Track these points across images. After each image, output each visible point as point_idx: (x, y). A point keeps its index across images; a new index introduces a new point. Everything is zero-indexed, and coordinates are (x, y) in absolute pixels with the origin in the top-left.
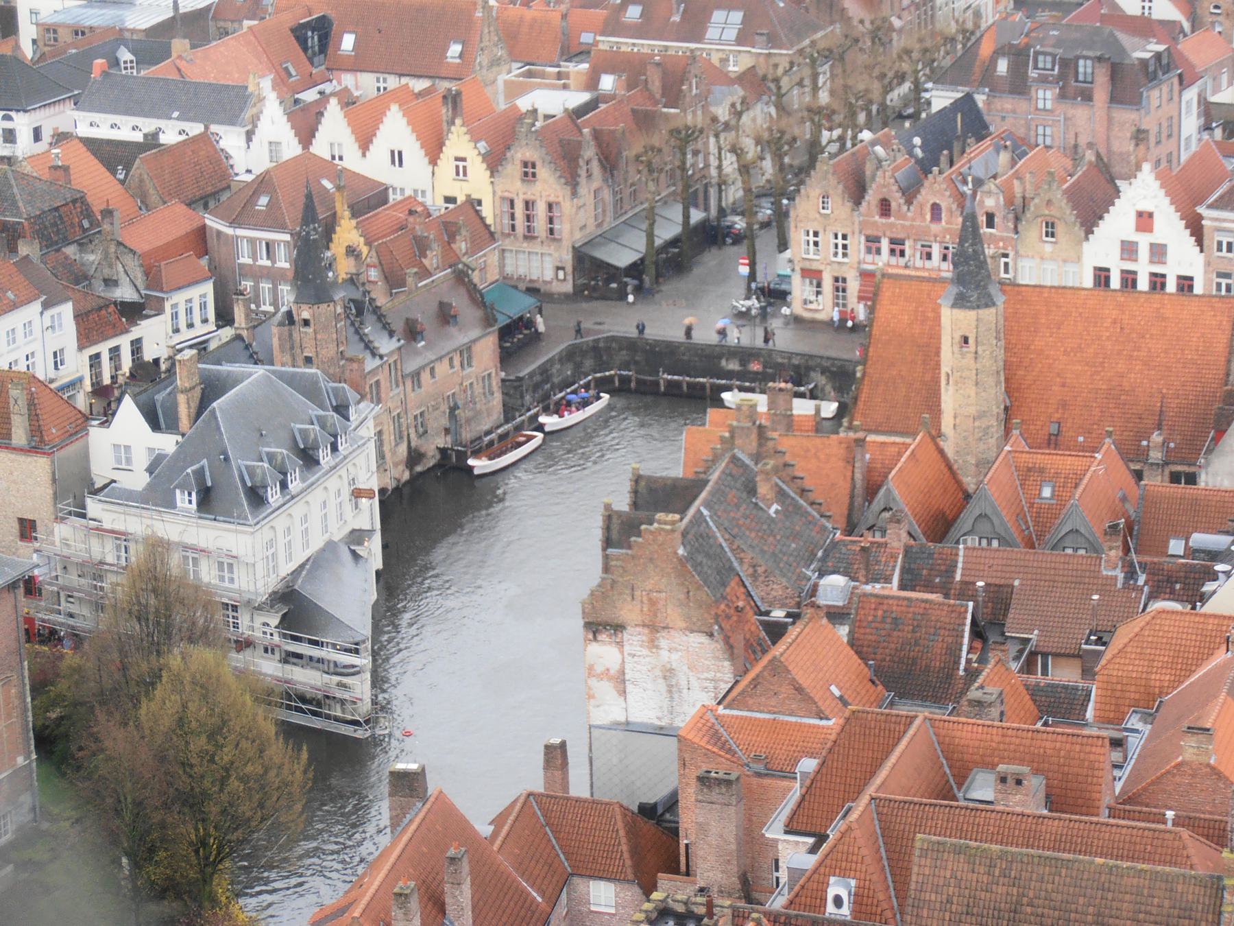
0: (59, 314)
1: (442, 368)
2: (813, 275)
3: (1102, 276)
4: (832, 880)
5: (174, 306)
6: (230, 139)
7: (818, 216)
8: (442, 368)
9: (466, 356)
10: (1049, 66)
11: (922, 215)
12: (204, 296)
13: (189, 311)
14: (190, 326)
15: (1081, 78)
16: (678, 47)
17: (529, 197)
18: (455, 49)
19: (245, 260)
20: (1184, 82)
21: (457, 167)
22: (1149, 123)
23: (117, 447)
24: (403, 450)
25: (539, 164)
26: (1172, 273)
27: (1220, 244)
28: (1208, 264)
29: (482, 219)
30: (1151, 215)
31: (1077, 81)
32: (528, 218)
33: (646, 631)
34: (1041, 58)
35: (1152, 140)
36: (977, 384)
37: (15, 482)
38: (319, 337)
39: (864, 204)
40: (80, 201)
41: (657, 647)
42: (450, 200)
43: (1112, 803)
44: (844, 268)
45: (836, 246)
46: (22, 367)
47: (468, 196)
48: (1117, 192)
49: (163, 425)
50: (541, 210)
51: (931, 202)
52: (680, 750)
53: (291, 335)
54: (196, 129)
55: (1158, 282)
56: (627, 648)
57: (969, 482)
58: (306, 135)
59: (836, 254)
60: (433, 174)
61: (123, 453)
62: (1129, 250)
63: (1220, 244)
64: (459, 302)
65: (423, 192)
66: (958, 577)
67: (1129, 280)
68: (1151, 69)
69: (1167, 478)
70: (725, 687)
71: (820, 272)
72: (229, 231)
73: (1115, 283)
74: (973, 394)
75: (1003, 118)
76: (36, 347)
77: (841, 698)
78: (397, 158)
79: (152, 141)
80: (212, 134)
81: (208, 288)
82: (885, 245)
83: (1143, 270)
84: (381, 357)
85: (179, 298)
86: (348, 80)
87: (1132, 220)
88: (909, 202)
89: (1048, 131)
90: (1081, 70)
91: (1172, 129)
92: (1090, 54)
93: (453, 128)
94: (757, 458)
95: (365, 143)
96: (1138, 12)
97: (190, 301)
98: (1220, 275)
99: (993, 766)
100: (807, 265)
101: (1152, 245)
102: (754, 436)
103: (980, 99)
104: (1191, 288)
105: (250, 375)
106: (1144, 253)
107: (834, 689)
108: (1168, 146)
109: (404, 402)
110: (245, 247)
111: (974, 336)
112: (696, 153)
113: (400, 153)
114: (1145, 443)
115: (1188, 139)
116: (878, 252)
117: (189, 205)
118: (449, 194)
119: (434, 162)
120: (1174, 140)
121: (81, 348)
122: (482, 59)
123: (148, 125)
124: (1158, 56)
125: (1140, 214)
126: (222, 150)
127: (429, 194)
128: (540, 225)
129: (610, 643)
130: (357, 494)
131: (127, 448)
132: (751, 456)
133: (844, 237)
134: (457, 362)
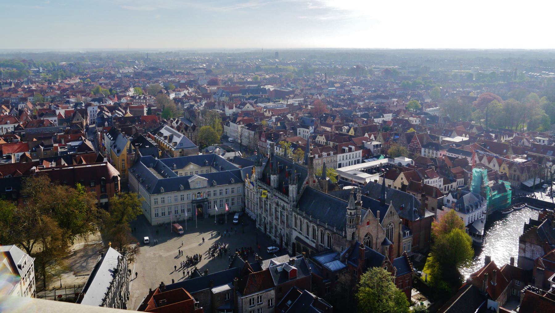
13: (460, 182)
16: (542, 155)
18: (505, 151)
23: (448, 200)
32: (514, 177)
40: (446, 165)
42: (502, 172)
46: (435, 186)
54: (464, 157)
61: (448, 201)
79: (457, 158)
85: (458, 180)
112: (543, 171)
121: (443, 185)
123: (457, 155)
130: (483, 213)
131: (449, 200)
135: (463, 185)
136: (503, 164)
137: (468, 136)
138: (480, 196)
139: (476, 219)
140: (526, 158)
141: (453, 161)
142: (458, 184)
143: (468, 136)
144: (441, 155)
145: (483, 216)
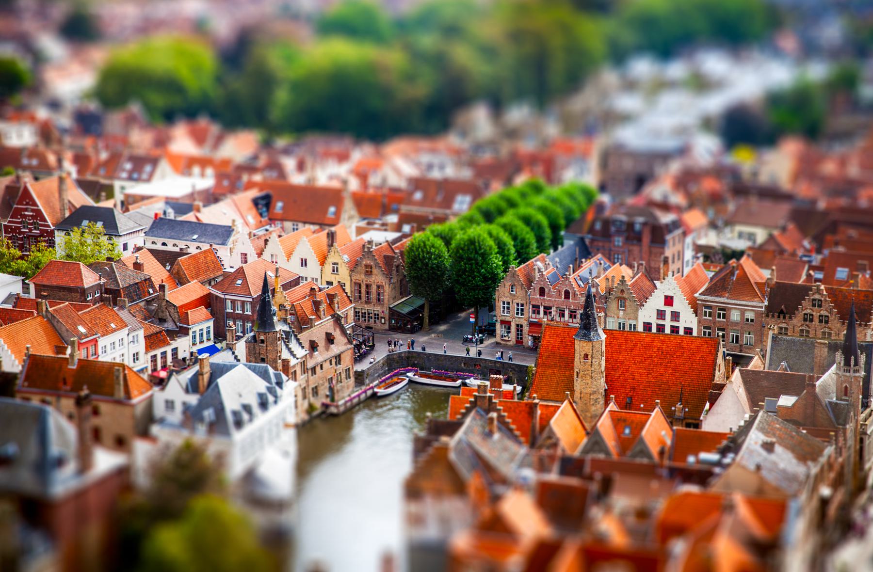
2: (506, 324)
3: (647, 326)
5: (194, 332)
6: (223, 252)
7: (509, 295)
9: (338, 359)
12: (209, 327)
13: (201, 335)
14: (201, 342)
17: (368, 282)
18: (332, 209)
20: (685, 234)
21: (333, 267)
24: (306, 405)
25: (374, 267)
26: (682, 325)
28: (699, 322)
30: (672, 298)
32: (368, 293)
35: (670, 261)
38: (268, 348)
42: (329, 283)
44: (522, 320)
45: (518, 309)
46: (118, 360)
47: (339, 282)
50: (374, 289)
51: (565, 289)
53: (254, 347)
54: (205, 247)
55: (675, 329)
59: (518, 314)
60: (322, 271)
61: (170, 405)
62: (661, 314)
63: (705, 312)
64: (337, 334)
65: (317, 280)
67: (661, 328)
71: (510, 322)
72: (222, 296)
73: (654, 330)
76: (125, 351)
78: (304, 263)
79: (182, 253)
80: (214, 249)
81: (211, 324)
82: (542, 309)
83: (668, 323)
84: (297, 359)
87: (662, 300)
89: (620, 257)
91: (680, 255)
97: (202, 330)
98: (705, 328)
100: (503, 318)
101: (672, 312)
103: (587, 241)
104: (691, 333)
106: (668, 316)
109: (307, 381)
110: (229, 304)
111: (591, 354)
115: (688, 262)
116: (539, 313)
117: (202, 283)
118: (329, 280)
121: (147, 351)
122: (344, 216)
126: (218, 257)
127: (319, 280)
128: (373, 296)
130: (287, 426)
133: (522, 305)
135: (211, 343)
138: (271, 371)
140: (398, 228)
141: (172, 265)
144: (125, 247)
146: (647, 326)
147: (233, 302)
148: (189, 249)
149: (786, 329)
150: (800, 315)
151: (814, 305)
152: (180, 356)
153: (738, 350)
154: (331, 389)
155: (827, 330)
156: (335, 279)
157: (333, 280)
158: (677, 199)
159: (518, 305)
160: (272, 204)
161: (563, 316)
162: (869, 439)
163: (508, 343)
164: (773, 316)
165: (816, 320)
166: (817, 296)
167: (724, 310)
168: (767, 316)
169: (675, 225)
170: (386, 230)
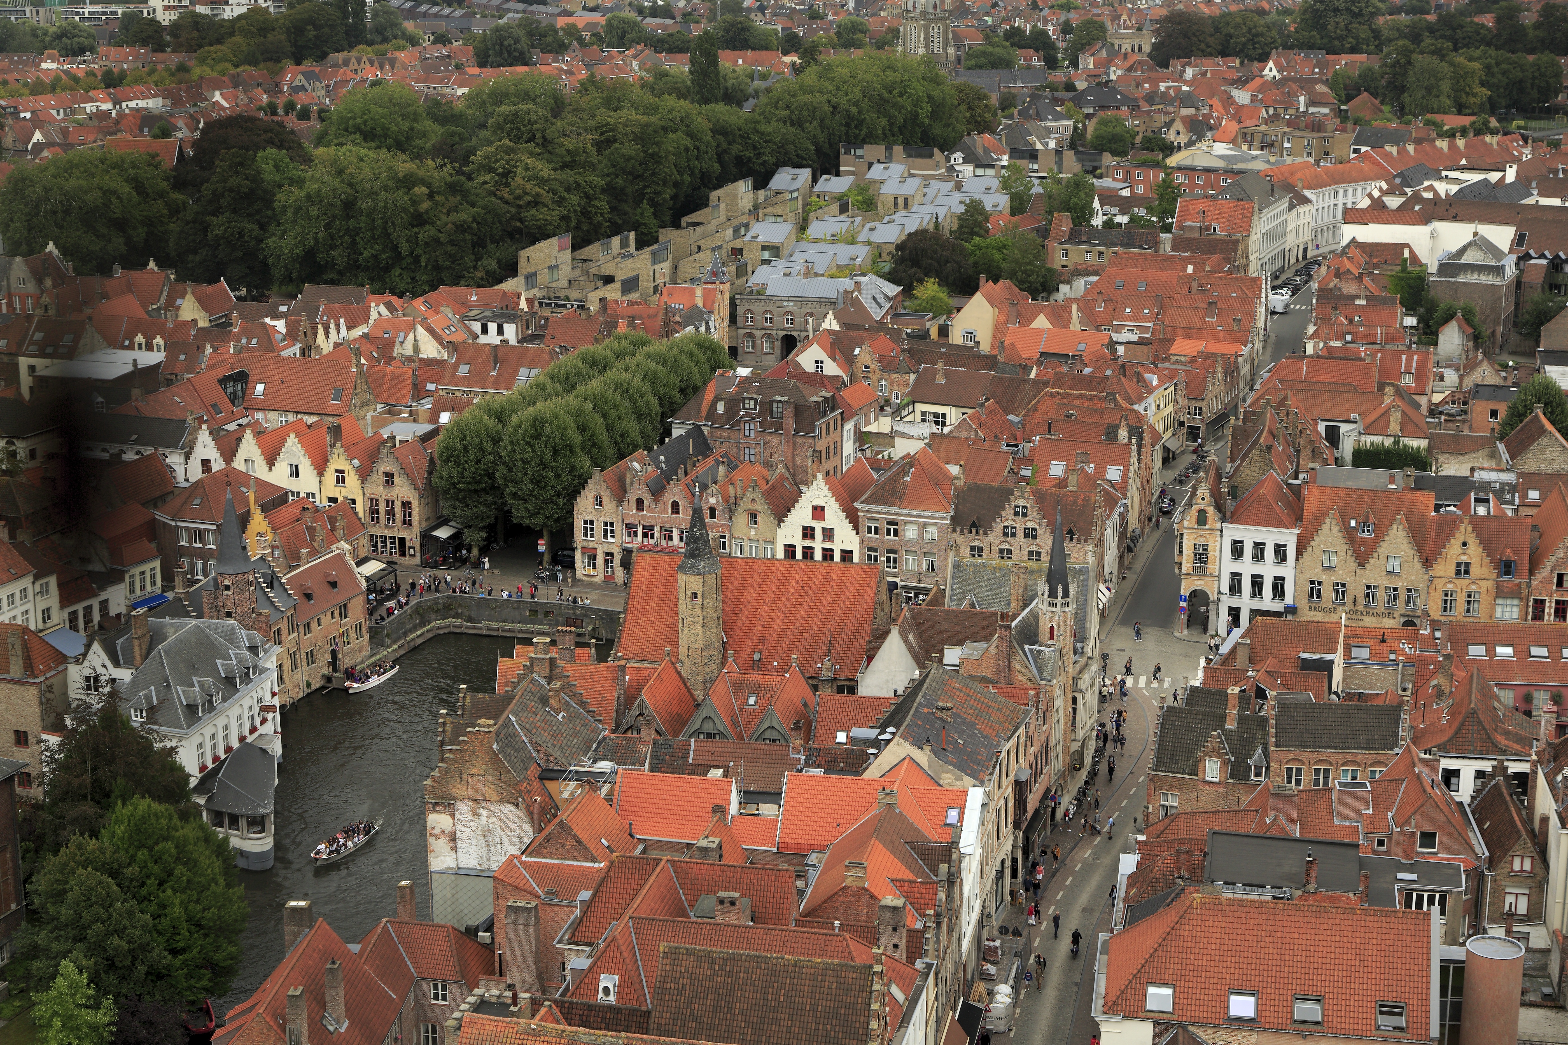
0: (47, 583)
1: (326, 619)
3: (790, 550)
4: (602, 976)
5: (132, 576)
8: (326, 619)
10: (752, 407)
11: (666, 508)
12: (153, 569)
15: (775, 415)
17: (389, 497)
19: (184, 543)
20: (844, 418)
22: (820, 446)
26: (837, 547)
27: (870, 527)
28: (862, 542)
29: (356, 514)
30: (823, 509)
31: (772, 417)
33: (469, 803)
34: (747, 401)
36: (703, 626)
37: (11, 704)
39: (626, 503)
41: (479, 815)
42: (333, 500)
43: (798, 917)
44: (613, 546)
45: (606, 531)
46: (19, 621)
47: (345, 498)
48: (800, 493)
49: (122, 662)
52: (495, 887)
55: (828, 554)
56: (457, 815)
57: (699, 694)
58: (229, 454)
62: (808, 532)
65: (314, 495)
66: (690, 761)
67: (808, 553)
68: (822, 408)
69: (835, 690)
70: (527, 842)
72: (173, 523)
73: (799, 555)
74: (701, 633)
75: (722, 442)
77: (608, 847)
78: (295, 471)
81: (157, 564)
83: (818, 545)
85: (136, 571)
86: (259, 416)
88: (656, 501)
89: (752, 452)
90: (775, 409)
92: (781, 398)
93: (335, 450)
94: (550, 680)
95: (271, 462)
96: (814, 370)
98: (870, 549)
99: (715, 893)
100: (586, 544)
102: (547, 664)
103: (706, 431)
104: (851, 559)
105: (187, 624)
106: (818, 533)
107: (603, 841)
108: (835, 461)
113: (297, 467)
114: (819, 666)
116: (636, 535)
118: (331, 496)
119: (321, 473)
120: (839, 457)
121: (62, 607)
124: (826, 399)
125: (815, 508)
127: (317, 496)
129: (445, 813)
130: (265, 709)
132: (544, 678)
133: (612, 525)
134: (337, 614)
136: (335, 456)
137: (158, 340)
139: (235, 745)
142: (132, 591)
143: (158, 340)
145: (264, 721)
146: (790, 550)
147: (187, 529)
148: (123, 456)
149: (980, 549)
150: (998, 529)
151: (1017, 514)
152: (113, 612)
153: (916, 580)
154: (334, 653)
155: (1035, 548)
156: (340, 494)
157: (337, 495)
158: (831, 368)
159: (606, 524)
160: (250, 383)
161: (671, 538)
162: (1083, 697)
163: (593, 579)
164: (962, 532)
165: (1020, 534)
166: (1021, 502)
167: (895, 524)
168: (954, 530)
169: (831, 404)
170: (415, 421)
